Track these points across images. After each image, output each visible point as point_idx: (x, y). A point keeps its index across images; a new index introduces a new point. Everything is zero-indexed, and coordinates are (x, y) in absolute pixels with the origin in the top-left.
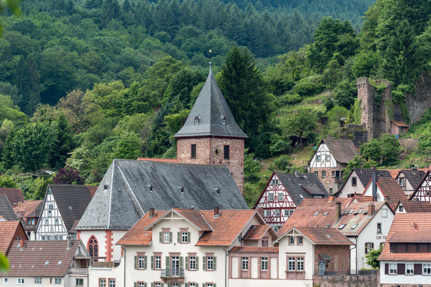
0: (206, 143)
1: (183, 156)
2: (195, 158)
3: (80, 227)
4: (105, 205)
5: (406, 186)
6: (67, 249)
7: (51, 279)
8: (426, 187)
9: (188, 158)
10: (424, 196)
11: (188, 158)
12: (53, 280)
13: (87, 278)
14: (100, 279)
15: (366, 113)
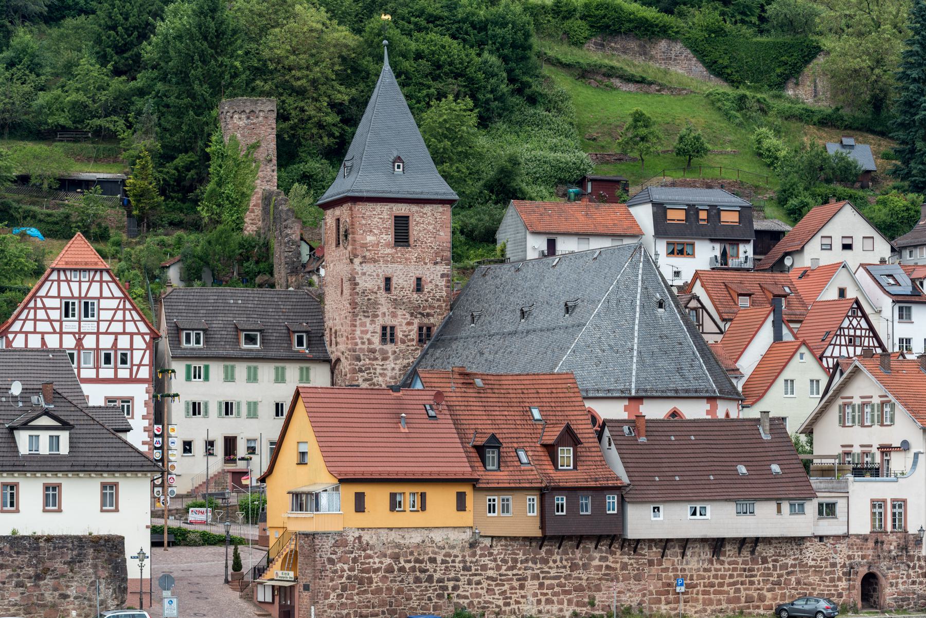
0: (438, 216)
1: (370, 238)
2: (409, 246)
3: (646, 391)
4: (680, 344)
5: (702, 325)
6: (763, 435)
7: (779, 505)
8: (848, 328)
9: (388, 245)
10: (846, 346)
11: (388, 245)
12: (786, 506)
13: (845, 500)
14: (872, 501)
15: (273, 171)
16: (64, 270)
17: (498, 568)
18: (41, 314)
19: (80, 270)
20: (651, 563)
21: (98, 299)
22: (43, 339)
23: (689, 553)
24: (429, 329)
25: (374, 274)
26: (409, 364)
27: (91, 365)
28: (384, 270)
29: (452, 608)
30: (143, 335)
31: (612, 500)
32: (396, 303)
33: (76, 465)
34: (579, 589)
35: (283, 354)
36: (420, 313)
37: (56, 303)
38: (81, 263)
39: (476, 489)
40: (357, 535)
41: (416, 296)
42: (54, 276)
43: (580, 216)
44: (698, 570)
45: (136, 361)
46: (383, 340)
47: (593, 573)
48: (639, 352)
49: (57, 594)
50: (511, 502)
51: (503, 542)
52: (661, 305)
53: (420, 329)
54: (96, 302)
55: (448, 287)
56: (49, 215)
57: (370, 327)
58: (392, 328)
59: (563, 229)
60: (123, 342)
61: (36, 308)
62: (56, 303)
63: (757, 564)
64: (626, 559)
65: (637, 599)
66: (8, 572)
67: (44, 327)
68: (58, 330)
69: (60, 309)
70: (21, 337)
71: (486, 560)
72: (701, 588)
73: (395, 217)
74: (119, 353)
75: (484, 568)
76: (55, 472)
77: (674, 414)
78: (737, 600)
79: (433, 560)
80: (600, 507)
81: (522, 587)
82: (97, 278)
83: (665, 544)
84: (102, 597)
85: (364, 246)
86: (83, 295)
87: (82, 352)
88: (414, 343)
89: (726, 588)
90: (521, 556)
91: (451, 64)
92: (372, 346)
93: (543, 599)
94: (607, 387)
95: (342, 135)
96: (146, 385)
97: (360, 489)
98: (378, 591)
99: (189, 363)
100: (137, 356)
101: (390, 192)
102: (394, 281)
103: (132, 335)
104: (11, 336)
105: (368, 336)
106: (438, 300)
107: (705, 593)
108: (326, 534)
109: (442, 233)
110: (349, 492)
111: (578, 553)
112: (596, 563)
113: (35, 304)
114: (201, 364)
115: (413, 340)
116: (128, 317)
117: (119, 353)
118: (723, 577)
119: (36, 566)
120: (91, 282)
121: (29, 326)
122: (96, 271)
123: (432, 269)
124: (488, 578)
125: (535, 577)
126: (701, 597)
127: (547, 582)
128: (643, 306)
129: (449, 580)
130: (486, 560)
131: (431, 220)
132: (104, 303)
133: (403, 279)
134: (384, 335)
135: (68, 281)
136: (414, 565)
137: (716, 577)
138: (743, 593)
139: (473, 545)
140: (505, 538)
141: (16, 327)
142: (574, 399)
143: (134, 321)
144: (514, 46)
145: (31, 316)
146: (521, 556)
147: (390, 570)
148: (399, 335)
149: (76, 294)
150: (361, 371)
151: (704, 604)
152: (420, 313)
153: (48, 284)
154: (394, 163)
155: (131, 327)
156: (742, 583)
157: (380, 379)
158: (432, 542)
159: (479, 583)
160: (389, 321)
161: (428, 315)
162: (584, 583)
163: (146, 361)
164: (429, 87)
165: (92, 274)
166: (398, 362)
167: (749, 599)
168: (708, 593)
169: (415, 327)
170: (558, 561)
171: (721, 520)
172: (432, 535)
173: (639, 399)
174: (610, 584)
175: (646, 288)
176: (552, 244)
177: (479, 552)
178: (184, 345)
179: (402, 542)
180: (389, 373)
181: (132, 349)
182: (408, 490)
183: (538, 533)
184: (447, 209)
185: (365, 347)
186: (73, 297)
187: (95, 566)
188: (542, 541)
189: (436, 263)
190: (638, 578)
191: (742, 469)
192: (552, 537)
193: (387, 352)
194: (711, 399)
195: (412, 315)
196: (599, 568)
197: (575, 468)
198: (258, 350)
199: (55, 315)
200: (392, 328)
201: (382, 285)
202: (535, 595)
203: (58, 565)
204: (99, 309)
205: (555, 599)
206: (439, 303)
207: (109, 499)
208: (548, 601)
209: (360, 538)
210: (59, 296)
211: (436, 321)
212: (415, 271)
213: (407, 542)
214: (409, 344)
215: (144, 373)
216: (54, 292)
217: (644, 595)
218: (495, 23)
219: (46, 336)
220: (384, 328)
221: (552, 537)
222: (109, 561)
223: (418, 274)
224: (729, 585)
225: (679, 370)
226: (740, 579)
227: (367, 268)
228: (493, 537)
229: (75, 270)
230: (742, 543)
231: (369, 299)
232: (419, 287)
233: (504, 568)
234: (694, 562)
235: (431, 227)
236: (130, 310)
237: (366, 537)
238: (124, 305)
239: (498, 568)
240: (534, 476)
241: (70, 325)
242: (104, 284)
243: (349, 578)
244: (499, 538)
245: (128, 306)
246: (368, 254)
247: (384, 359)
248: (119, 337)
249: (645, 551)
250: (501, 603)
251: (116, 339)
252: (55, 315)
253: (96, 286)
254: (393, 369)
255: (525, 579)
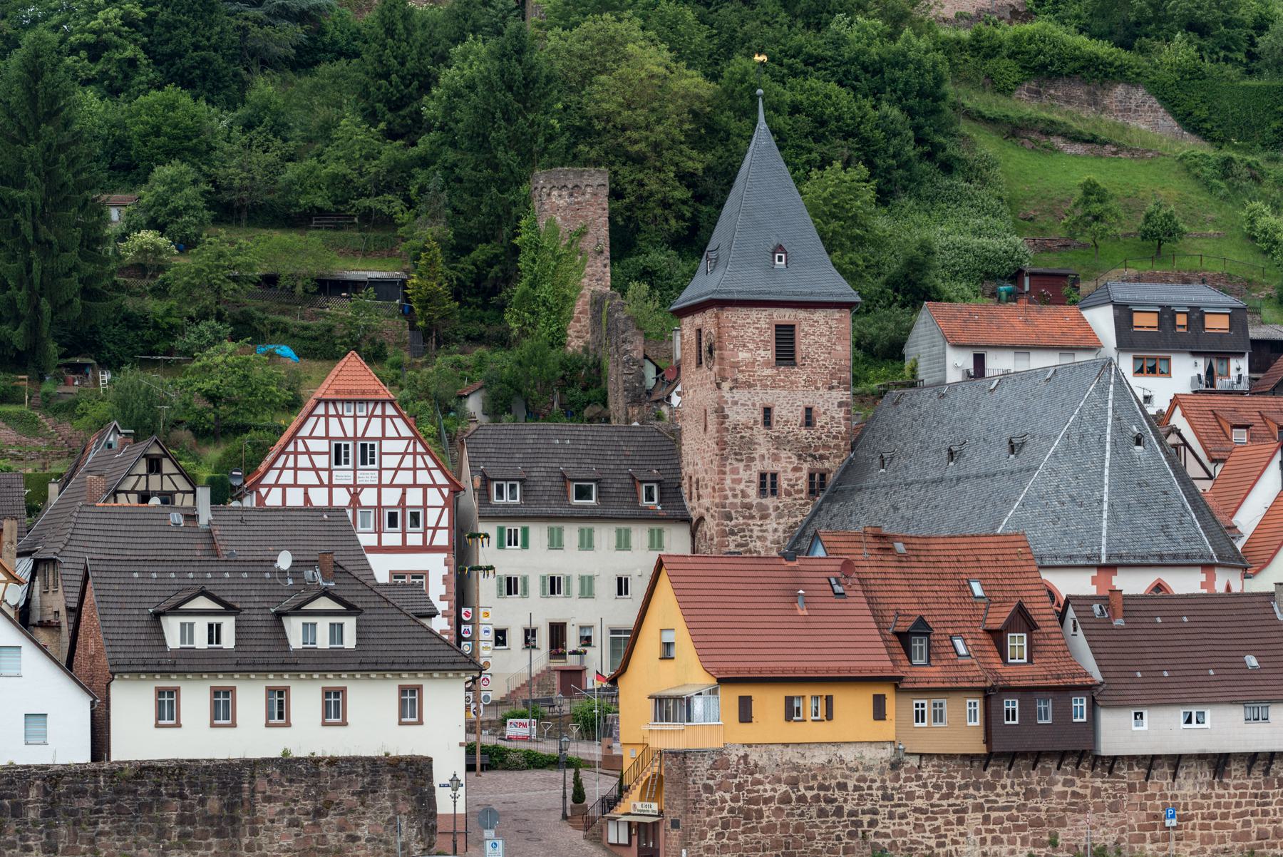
1: (743, 355)
2: (795, 364)
3: (1121, 557)
4: (1165, 493)
9: (766, 364)
11: (766, 364)
15: (605, 266)
16: (334, 402)
17: (929, 796)
18: (303, 461)
19: (355, 401)
20: (1132, 788)
21: (380, 439)
22: (306, 493)
23: (1182, 774)
24: (823, 476)
25: (749, 403)
26: (796, 523)
27: (371, 529)
28: (762, 397)
29: (868, 851)
30: (439, 487)
31: (1080, 704)
32: (778, 442)
33: (365, 663)
34: (1037, 823)
35: (628, 511)
36: (811, 455)
37: (323, 446)
38: (356, 391)
39: (899, 690)
40: (741, 753)
41: (804, 432)
42: (321, 410)
43: (1017, 322)
44: (1195, 796)
45: (431, 523)
46: (762, 492)
47: (1054, 802)
48: (1111, 505)
49: (343, 835)
50: (945, 707)
51: (935, 762)
52: (1138, 443)
53: (811, 476)
54: (376, 444)
55: (848, 419)
56: (306, 328)
57: (744, 475)
58: (774, 476)
59: (994, 341)
60: (414, 497)
61: (296, 453)
62: (323, 446)
63: (1273, 788)
64: (1098, 783)
65: (1113, 836)
66: (278, 806)
67: (307, 478)
68: (326, 482)
69: (329, 453)
70: (276, 492)
71: (912, 786)
72: (1198, 821)
73: (777, 326)
74: (408, 512)
75: (911, 796)
76: (338, 672)
77: (1159, 587)
78: (1246, 836)
79: (842, 787)
80: (1063, 713)
81: (961, 821)
82: (378, 411)
83: (1150, 762)
84: (403, 839)
85: (735, 365)
86: (359, 435)
87: (359, 511)
88: (803, 495)
89: (1231, 821)
90: (959, 780)
91: (839, 119)
92: (747, 500)
93: (989, 837)
94: (1068, 551)
95: (694, 218)
96: (445, 555)
97: (745, 691)
98: (771, 828)
99: (501, 524)
100: (433, 516)
101: (769, 293)
102: (776, 413)
103: (425, 487)
104: (263, 491)
105: (742, 486)
106: (835, 437)
107: (1203, 827)
108: (701, 753)
109: (839, 348)
110: (731, 696)
111: (1035, 775)
112: (1059, 788)
113: (296, 447)
114: (518, 526)
115: (801, 491)
116: (420, 464)
117: (408, 512)
118: (1227, 806)
119: (315, 798)
120: (370, 417)
121: (287, 477)
122: (376, 402)
123: (826, 396)
124: (916, 810)
125: (978, 808)
126: (1198, 832)
127: (994, 815)
128: (1114, 443)
129: (864, 813)
130: (912, 786)
131: (824, 329)
132: (387, 446)
133: (788, 409)
134: (763, 485)
135: (339, 416)
136: (818, 793)
137: (1217, 805)
138: (1254, 827)
139: (895, 766)
140: (938, 755)
141: (271, 478)
142: (1026, 569)
143: (429, 469)
144: (922, 94)
145: (290, 463)
146: (959, 780)
147: (785, 799)
148: (783, 484)
149: (350, 434)
150: (732, 533)
151: (1202, 842)
152: (811, 455)
153: (312, 420)
154: (774, 253)
155: (423, 477)
156: (1253, 814)
157: (759, 544)
158: (842, 761)
159: (903, 816)
160: (769, 466)
161: (822, 457)
162: (1043, 816)
163: (445, 522)
164: (810, 151)
165: (371, 406)
166: (782, 521)
167: (1262, 835)
168: (1207, 827)
169: (804, 474)
170: (1007, 786)
171: (1225, 728)
172: (841, 752)
173: (1111, 568)
174: (1078, 816)
175: (1119, 419)
176: (979, 361)
177: (903, 775)
178: (495, 500)
179: (802, 762)
180: (770, 537)
181: (425, 507)
182: (808, 692)
183: (981, 749)
184: (846, 314)
185: (738, 501)
186: (346, 438)
187: (394, 798)
188: (986, 759)
189: (831, 388)
190: (1114, 808)
191: (1252, 661)
192: (1000, 753)
193: (767, 508)
194: (1207, 567)
195: (800, 457)
196: (1063, 795)
197: (1030, 660)
198: (593, 507)
199: (322, 462)
200: (774, 476)
201: (760, 418)
202: (978, 832)
203: (345, 796)
204: (381, 453)
205: (1004, 837)
206: (836, 441)
207: (410, 708)
208: (996, 841)
209: (745, 757)
210: (327, 437)
211: (832, 465)
212: (804, 398)
213: (808, 762)
214: (797, 496)
215: (442, 538)
216: (320, 431)
217: (1123, 831)
218: (895, 65)
219: (310, 490)
220: (763, 476)
221: (1000, 753)
222: (413, 790)
223: (808, 402)
224: (1236, 816)
225: (1164, 528)
226: (1250, 808)
227: (741, 395)
228: (921, 755)
229: (349, 401)
230: (1252, 759)
231: (742, 437)
232: (809, 420)
233: (937, 796)
234: (1189, 787)
235: (824, 340)
236: (422, 454)
237: (754, 757)
238: (415, 448)
239: (929, 796)
240: (975, 673)
241: (343, 475)
242: (388, 420)
243: (732, 811)
244: (930, 756)
245: (420, 449)
246: (740, 376)
247: (763, 517)
248: (409, 490)
249: (1124, 772)
250: (933, 843)
251: (404, 494)
252: (322, 462)
253: (376, 423)
254: (776, 530)
255: (965, 811)
